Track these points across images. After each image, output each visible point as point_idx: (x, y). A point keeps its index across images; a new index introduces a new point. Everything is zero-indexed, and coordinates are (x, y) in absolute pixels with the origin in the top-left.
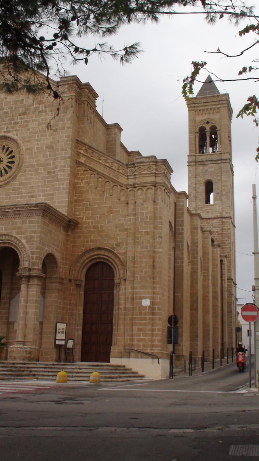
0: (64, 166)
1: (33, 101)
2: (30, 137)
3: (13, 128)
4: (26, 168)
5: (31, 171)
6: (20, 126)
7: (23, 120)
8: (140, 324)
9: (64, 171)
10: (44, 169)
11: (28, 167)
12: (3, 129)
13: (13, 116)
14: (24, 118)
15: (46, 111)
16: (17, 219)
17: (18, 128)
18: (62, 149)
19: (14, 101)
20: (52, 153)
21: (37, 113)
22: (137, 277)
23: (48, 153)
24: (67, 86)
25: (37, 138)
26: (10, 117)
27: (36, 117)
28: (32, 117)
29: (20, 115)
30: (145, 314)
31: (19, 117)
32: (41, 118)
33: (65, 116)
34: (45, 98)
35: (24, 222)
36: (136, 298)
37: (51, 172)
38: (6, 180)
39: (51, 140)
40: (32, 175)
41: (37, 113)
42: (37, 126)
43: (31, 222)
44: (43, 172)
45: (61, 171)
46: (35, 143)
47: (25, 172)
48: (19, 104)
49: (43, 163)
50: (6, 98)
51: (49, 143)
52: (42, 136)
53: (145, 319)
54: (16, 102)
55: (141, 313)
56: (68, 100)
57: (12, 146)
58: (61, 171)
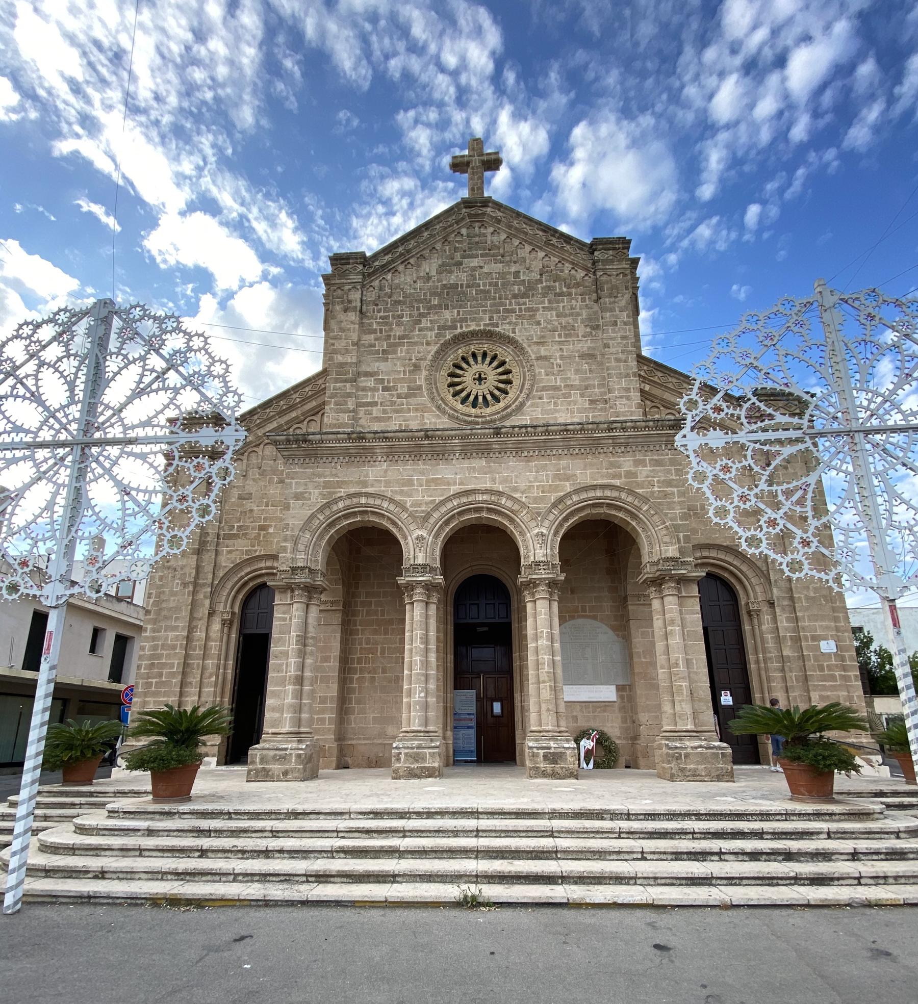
0: (628, 390)
1: (541, 275)
2: (543, 337)
3: (505, 319)
4: (541, 391)
5: (553, 398)
6: (520, 316)
7: (523, 307)
8: (824, 688)
9: (628, 398)
10: (582, 395)
11: (547, 390)
12: (481, 319)
13: (500, 298)
14: (525, 304)
15: (570, 294)
16: (619, 457)
17: (514, 320)
18: (618, 360)
19: (499, 273)
20: (594, 367)
21: (551, 296)
22: (799, 598)
23: (586, 367)
24: (611, 252)
25: (557, 339)
26: (494, 299)
27: (550, 302)
28: (543, 302)
29: (515, 296)
30: (830, 668)
31: (513, 301)
32: (561, 305)
33: (614, 302)
34: (567, 272)
35: (637, 463)
36: (806, 638)
37: (597, 400)
38: (499, 413)
39: (589, 344)
40: (556, 404)
41: (551, 296)
42: (555, 318)
43: (658, 463)
44: (579, 399)
45: (621, 397)
46: (556, 347)
47: (540, 398)
48: (511, 278)
49: (577, 383)
50: (481, 267)
51: (585, 349)
52: (566, 336)
53: (833, 678)
54: (502, 275)
55: (821, 668)
56: (617, 275)
57: (505, 353)
58: (621, 397)
